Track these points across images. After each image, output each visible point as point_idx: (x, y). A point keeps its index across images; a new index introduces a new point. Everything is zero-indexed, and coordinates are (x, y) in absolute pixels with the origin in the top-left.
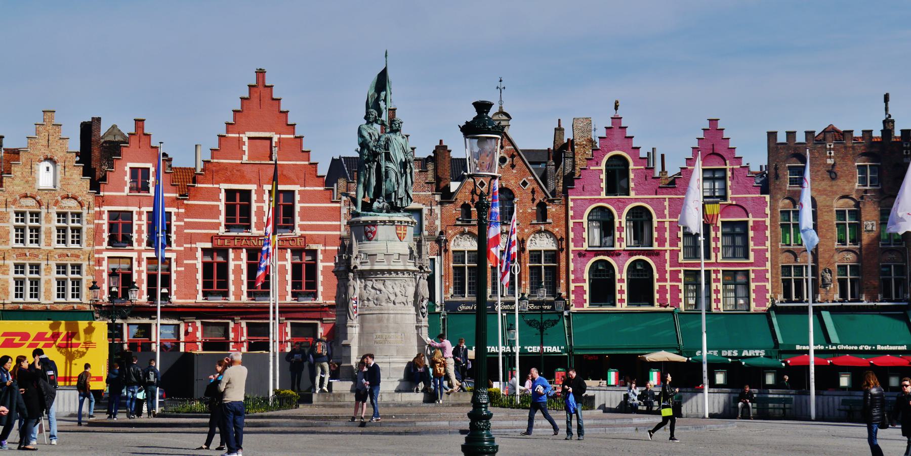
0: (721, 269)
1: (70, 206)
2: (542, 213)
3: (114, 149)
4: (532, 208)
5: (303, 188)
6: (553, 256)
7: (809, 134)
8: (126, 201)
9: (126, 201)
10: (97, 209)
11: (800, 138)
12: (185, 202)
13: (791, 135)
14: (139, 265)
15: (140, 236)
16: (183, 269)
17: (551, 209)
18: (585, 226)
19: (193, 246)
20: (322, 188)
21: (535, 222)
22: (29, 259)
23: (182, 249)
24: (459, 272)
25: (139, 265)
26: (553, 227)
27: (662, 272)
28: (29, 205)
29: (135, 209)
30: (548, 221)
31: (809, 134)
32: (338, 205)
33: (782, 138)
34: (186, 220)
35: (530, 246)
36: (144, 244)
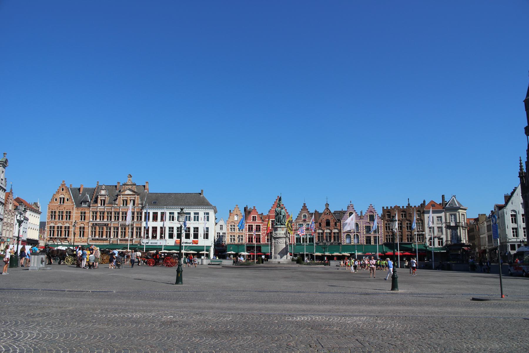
2: (336, 224)
3: (250, 212)
4: (334, 223)
6: (338, 233)
7: (391, 207)
8: (251, 223)
9: (251, 223)
11: (389, 208)
13: (387, 207)
17: (338, 223)
24: (319, 237)
27: (361, 236)
28: (233, 224)
31: (391, 207)
33: (385, 208)
35: (333, 231)
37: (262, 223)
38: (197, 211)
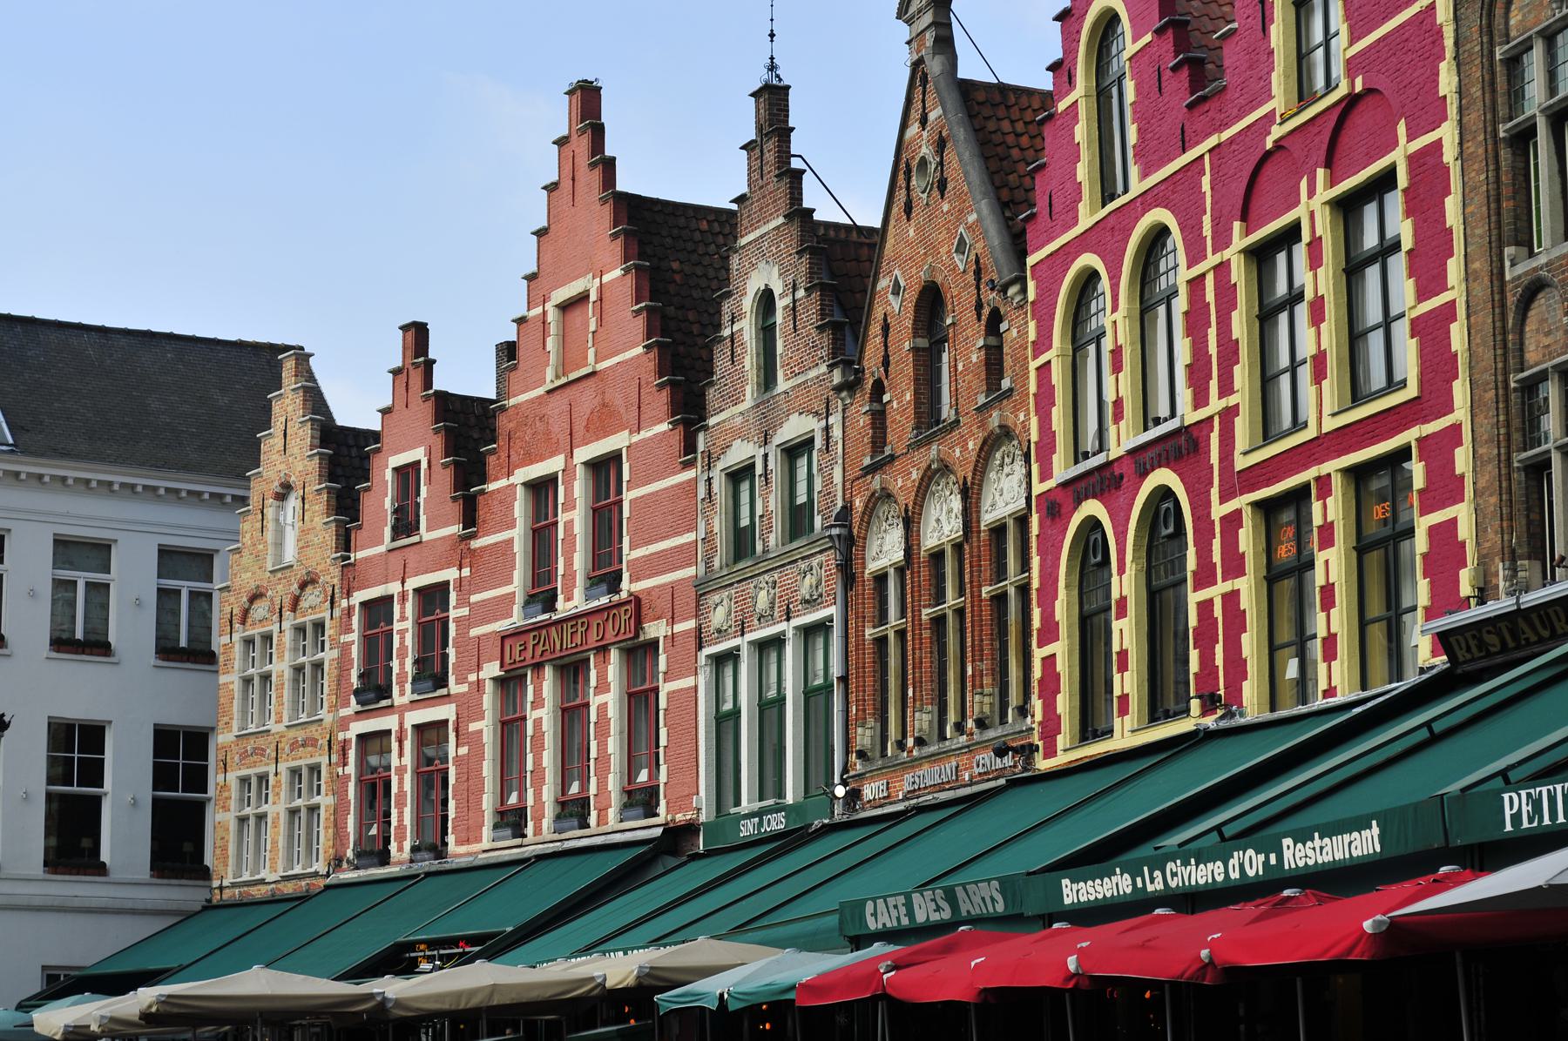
0: (1332, 466)
1: (314, 604)
5: (636, 438)
10: (344, 603)
12: (476, 544)
14: (401, 755)
15: (402, 665)
16: (463, 750)
18: (1058, 376)
19: (482, 675)
20: (664, 427)
21: (982, 399)
22: (254, 765)
23: (464, 688)
25: (401, 755)
26: (1015, 411)
29: (394, 588)
30: (1006, 384)
32: (690, 474)
34: (474, 598)
36: (409, 696)
37: (460, 552)
38: (87, 515)
